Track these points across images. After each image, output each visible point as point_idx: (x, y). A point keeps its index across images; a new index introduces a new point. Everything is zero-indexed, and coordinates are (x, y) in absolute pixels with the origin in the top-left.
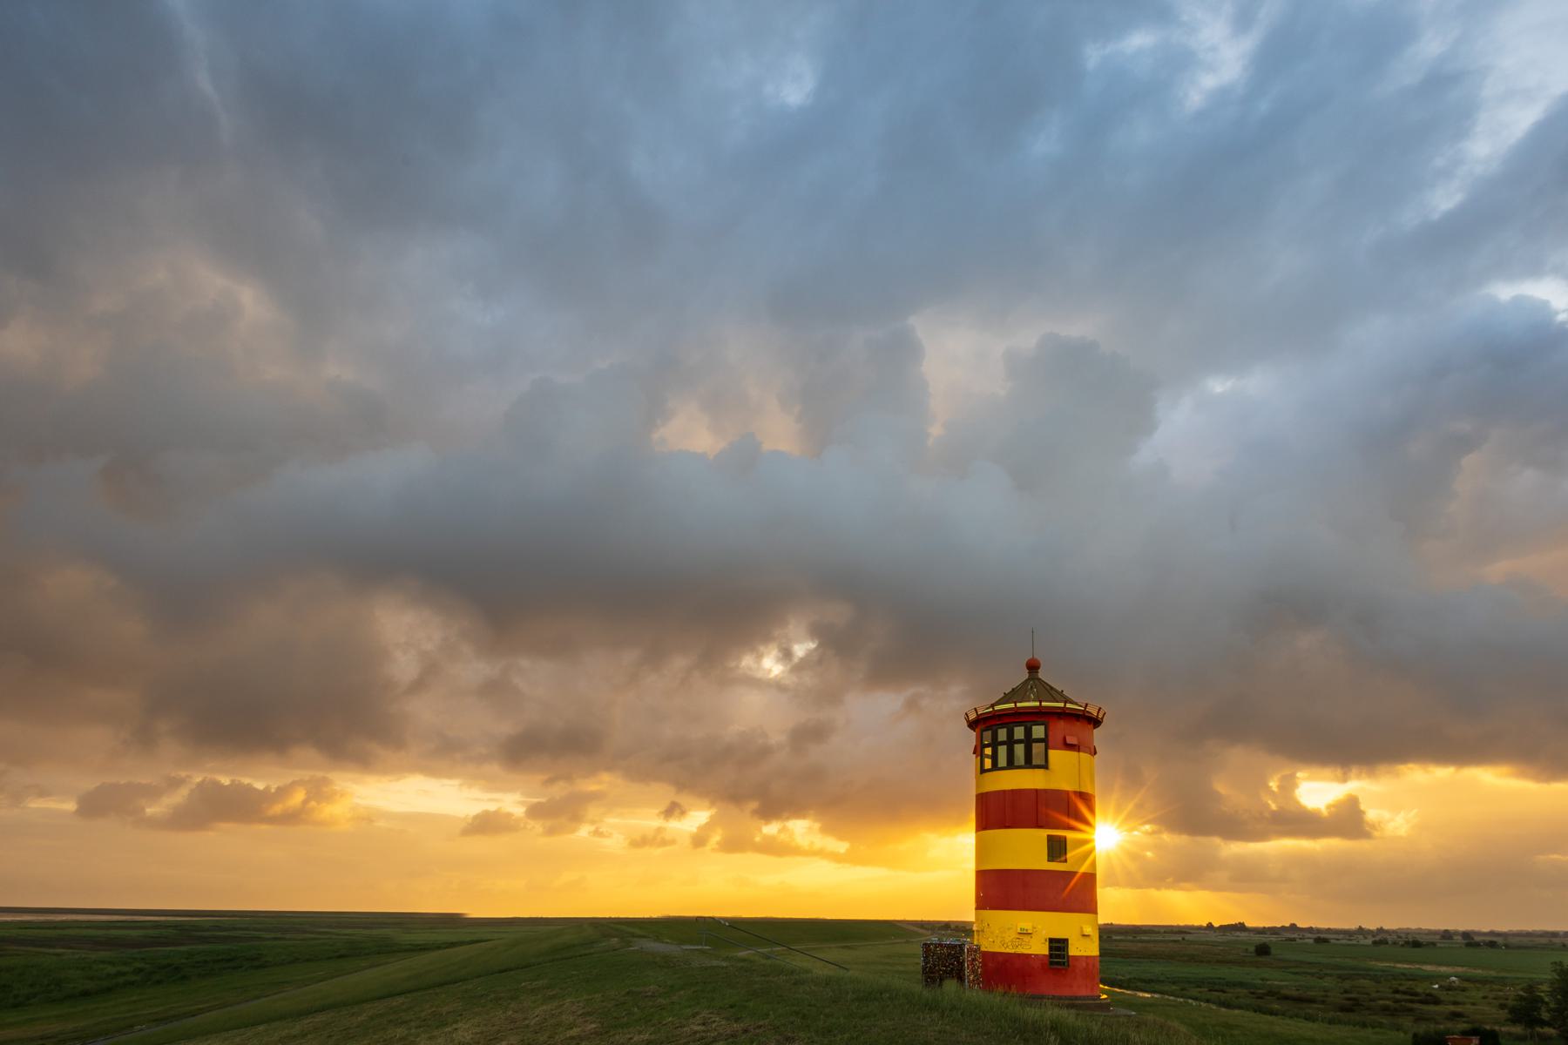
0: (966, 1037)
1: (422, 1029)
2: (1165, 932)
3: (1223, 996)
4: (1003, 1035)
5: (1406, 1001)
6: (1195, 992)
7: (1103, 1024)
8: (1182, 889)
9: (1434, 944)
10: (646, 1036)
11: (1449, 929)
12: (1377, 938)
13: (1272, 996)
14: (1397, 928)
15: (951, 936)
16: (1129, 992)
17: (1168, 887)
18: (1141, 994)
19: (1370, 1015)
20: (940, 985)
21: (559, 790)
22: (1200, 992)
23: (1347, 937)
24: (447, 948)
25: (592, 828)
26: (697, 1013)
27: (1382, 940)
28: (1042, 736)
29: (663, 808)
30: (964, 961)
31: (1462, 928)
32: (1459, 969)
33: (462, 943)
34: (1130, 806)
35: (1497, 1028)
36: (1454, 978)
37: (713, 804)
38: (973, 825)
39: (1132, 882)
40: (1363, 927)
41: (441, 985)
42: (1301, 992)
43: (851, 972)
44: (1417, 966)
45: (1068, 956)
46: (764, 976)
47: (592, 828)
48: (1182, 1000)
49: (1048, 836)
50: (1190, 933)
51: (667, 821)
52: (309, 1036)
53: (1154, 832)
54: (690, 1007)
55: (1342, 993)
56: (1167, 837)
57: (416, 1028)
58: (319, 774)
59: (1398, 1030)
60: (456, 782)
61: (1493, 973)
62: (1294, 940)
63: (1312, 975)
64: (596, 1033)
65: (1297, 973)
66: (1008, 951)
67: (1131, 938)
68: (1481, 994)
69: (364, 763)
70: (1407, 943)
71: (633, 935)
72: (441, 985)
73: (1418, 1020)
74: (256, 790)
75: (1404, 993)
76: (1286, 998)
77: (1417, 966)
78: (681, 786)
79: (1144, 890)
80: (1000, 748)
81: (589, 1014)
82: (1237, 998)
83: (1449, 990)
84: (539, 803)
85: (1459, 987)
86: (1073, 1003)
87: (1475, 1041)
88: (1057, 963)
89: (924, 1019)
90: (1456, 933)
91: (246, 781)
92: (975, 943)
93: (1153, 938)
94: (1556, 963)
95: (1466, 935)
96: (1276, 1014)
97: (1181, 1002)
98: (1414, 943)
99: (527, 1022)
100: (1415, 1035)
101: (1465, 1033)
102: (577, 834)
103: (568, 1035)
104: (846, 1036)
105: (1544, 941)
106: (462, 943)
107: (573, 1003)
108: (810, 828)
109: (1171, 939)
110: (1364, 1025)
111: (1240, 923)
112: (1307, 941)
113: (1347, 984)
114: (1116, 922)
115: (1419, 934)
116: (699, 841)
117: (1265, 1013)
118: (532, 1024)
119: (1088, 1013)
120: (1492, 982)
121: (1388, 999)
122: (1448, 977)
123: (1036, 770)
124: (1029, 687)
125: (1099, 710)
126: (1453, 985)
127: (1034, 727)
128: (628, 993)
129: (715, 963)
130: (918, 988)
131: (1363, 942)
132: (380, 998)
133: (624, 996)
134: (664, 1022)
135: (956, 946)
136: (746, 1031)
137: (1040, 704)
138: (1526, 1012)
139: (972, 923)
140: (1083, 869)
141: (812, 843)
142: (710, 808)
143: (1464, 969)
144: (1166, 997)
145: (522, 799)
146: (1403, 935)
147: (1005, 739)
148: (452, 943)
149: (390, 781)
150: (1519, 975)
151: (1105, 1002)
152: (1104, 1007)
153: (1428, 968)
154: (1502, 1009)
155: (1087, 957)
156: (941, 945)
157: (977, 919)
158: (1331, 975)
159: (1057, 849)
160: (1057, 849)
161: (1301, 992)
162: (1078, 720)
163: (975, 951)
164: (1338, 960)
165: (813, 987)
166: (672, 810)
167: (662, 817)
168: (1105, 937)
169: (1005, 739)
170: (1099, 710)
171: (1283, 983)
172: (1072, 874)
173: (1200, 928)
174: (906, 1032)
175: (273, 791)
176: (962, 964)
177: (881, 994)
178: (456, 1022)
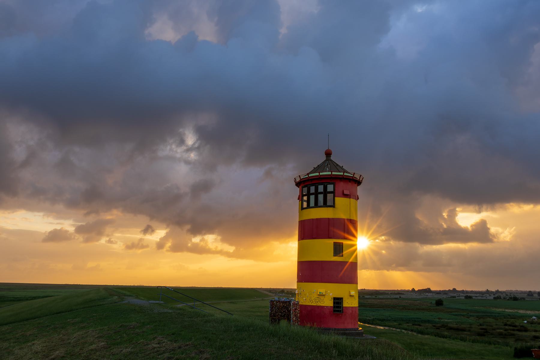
1: (16, 344)
2: (391, 294)
3: (420, 328)
4: (309, 350)
5: (511, 330)
6: (405, 326)
9: (524, 299)
10: (129, 350)
11: (531, 290)
12: (496, 296)
13: (444, 328)
14: (505, 290)
15: (284, 296)
16: (373, 326)
17: (393, 270)
18: (379, 327)
19: (493, 337)
20: (279, 323)
21: (92, 219)
22: (408, 326)
24: (31, 300)
26: (156, 337)
27: (498, 296)
28: (332, 190)
29: (143, 228)
30: (290, 310)
32: (537, 312)
33: (39, 297)
34: (375, 226)
36: (534, 317)
37: (168, 226)
38: (296, 237)
39: (375, 267)
41: (27, 320)
42: (458, 325)
43: (234, 316)
44: (516, 311)
45: (343, 307)
46: (190, 317)
47: (108, 239)
49: (334, 243)
50: (403, 294)
51: (145, 235)
53: (386, 240)
54: (152, 334)
55: (478, 326)
56: (392, 242)
59: (507, 346)
60: (41, 214)
62: (455, 297)
63: (463, 315)
64: (104, 347)
66: (313, 304)
67: (374, 297)
70: (511, 298)
71: (125, 295)
72: (27, 320)
73: (517, 340)
75: (510, 325)
76: (451, 328)
77: (516, 311)
78: (152, 217)
79: (381, 271)
81: (101, 337)
82: (426, 329)
84: (82, 226)
85: (537, 322)
86: (345, 333)
88: (338, 311)
90: (535, 292)
92: (297, 300)
93: (385, 297)
96: (446, 338)
97: (398, 331)
99: (69, 341)
100: (516, 349)
102: (99, 242)
103: (90, 348)
104: (231, 350)
106: (39, 297)
107: (93, 331)
108: (215, 239)
109: (394, 297)
110: (490, 343)
111: (428, 288)
112: (461, 297)
113: (481, 321)
114: (366, 288)
115: (517, 293)
116: (160, 246)
117: (440, 337)
118: (72, 342)
119: (352, 338)
121: (501, 329)
122: (531, 316)
124: (326, 164)
125: (360, 176)
126: (534, 320)
128: (121, 326)
129: (166, 310)
130: (267, 324)
131: (489, 298)
133: (119, 328)
134: (139, 342)
135: (287, 302)
136: (180, 347)
137: (332, 173)
139: (295, 290)
140: (351, 260)
141: (217, 247)
142: (166, 228)
144: (391, 328)
145: (73, 223)
146: (508, 294)
147: (314, 192)
148: (34, 297)
149: (9, 213)
151: (361, 331)
152: (360, 334)
153: (521, 312)
155: (352, 307)
156: (279, 301)
157: (298, 287)
158: (473, 316)
160: (338, 249)
161: (458, 325)
162: (350, 182)
163: (297, 305)
164: (476, 307)
165: (214, 324)
166: (148, 230)
167: (143, 232)
169: (314, 192)
170: (360, 176)
171: (449, 321)
172: (344, 263)
173: (408, 291)
176: (289, 311)
178: (34, 340)
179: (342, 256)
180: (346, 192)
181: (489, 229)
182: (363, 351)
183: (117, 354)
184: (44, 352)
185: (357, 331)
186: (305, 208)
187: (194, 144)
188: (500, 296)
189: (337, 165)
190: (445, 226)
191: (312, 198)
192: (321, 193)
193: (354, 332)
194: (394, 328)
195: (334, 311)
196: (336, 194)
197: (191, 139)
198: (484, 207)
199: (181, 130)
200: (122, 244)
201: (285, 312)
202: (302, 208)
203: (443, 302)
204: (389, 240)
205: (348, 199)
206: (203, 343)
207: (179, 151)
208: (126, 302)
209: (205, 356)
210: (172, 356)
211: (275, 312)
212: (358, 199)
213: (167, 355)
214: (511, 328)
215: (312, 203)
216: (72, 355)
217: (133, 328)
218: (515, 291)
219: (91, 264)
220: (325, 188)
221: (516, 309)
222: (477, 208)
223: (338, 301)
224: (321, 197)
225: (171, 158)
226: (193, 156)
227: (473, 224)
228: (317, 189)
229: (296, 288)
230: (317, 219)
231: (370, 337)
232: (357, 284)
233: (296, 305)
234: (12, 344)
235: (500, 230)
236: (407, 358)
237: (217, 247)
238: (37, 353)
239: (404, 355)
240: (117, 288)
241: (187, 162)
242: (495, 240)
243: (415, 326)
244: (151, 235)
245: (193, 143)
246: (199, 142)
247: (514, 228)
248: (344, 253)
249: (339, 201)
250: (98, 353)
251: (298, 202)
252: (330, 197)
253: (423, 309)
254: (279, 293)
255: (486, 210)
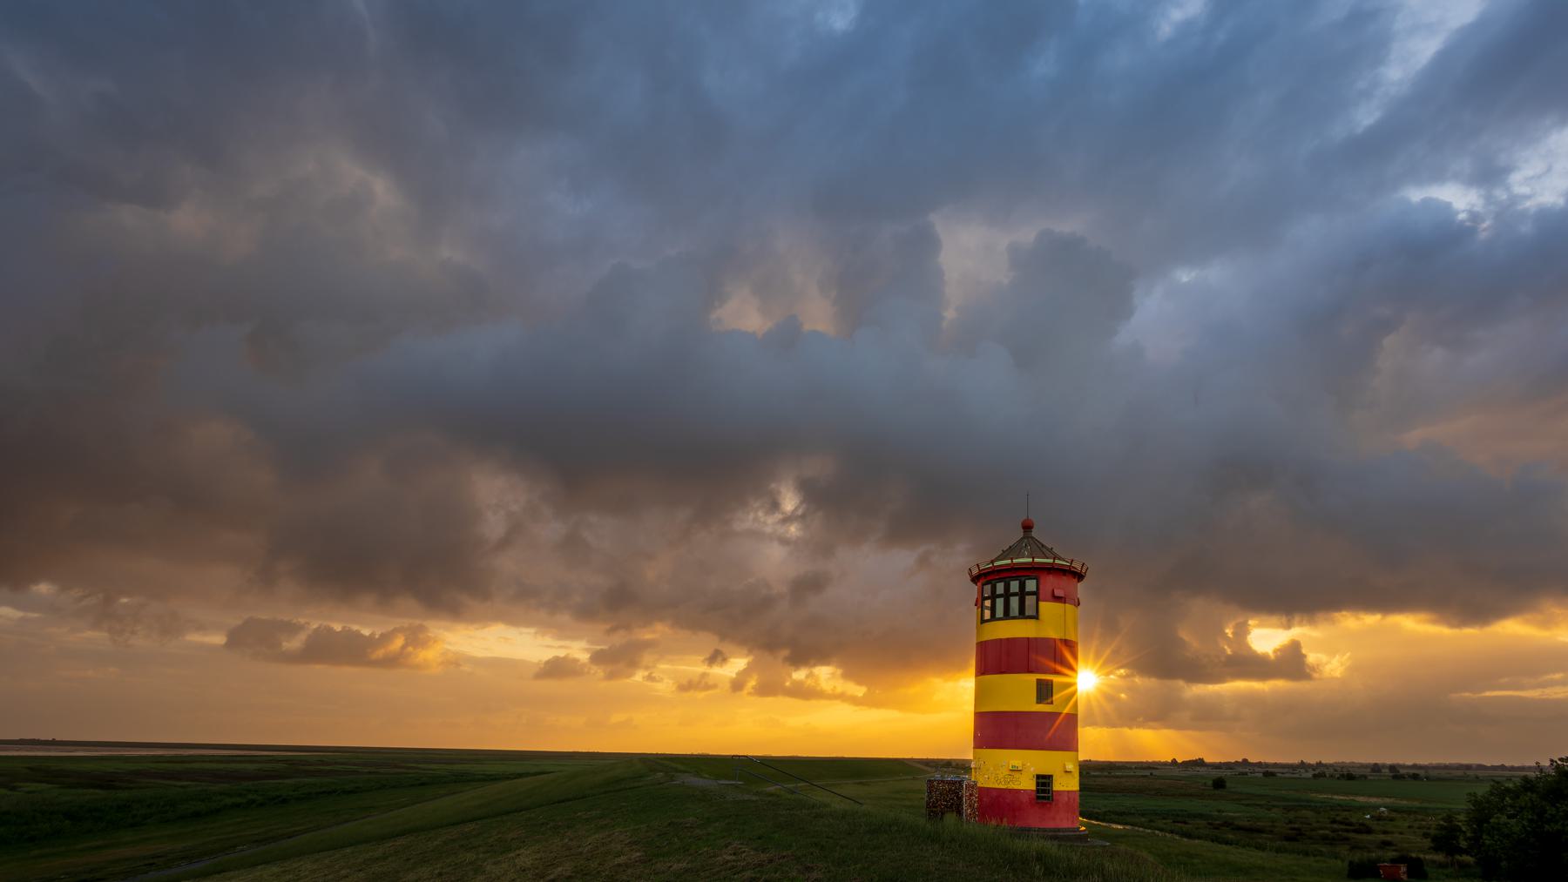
0: (963, 867)
1: (489, 854)
2: (1136, 768)
3: (1185, 827)
4: (995, 865)
5: (1342, 830)
7: (1082, 854)
8: (1149, 728)
11: (1378, 762)
12: (1317, 772)
16: (1104, 824)
17: (1139, 726)
18: (1114, 826)
20: (942, 819)
21: (619, 639)
22: (1165, 824)
23: (1291, 771)
25: (646, 673)
26: (730, 844)
27: (1321, 773)
29: (708, 656)
31: (1389, 762)
32: (1388, 800)
34: (1108, 652)
35: (1422, 856)
36: (1383, 809)
37: (750, 652)
38: (972, 670)
39: (1109, 723)
40: (1305, 761)
41: (508, 813)
47: (646, 673)
48: (1149, 831)
49: (1038, 680)
50: (1157, 769)
52: (390, 859)
53: (1127, 676)
54: (724, 837)
56: (1137, 680)
57: (484, 853)
58: (417, 622)
59: (1336, 858)
60: (532, 630)
61: (1417, 804)
62: (1246, 774)
65: (1248, 805)
66: (1001, 786)
67: (1106, 774)
68: (1406, 824)
69: (455, 612)
70: (1343, 776)
71: (677, 771)
72: (508, 813)
73: (1354, 848)
74: (362, 636)
75: (1341, 823)
76: (1239, 828)
78: (723, 636)
80: (998, 600)
81: (635, 843)
82: (1197, 829)
83: (1379, 820)
84: (602, 650)
87: (1403, 868)
88: (1044, 798)
89: (927, 850)
90: (1384, 766)
91: (355, 627)
92: (973, 780)
93: (1125, 774)
94: (1470, 794)
95: (1393, 768)
96: (1231, 844)
97: (1149, 833)
98: (1348, 776)
99: (580, 850)
100: (1351, 863)
101: (1393, 861)
102: (633, 678)
104: (859, 866)
105: (1460, 773)
106: (527, 775)
108: (833, 674)
110: (1307, 854)
113: (1292, 815)
116: (737, 685)
117: (1220, 843)
119: (1069, 844)
120: (1415, 812)
121: (1326, 829)
123: (1028, 620)
127: (1027, 581)
128: (669, 824)
129: (746, 797)
132: (453, 824)
136: (771, 861)
138: (1445, 840)
139: (969, 761)
140: (1066, 711)
141: (835, 687)
142: (747, 655)
143: (1392, 800)
144: (1136, 828)
145: (587, 646)
146: (1339, 769)
149: (477, 629)
150: (1439, 805)
151: (1082, 833)
152: (1082, 838)
153: (1361, 799)
154: (1426, 838)
155: (1068, 791)
159: (1045, 691)
160: (1045, 691)
162: (1065, 575)
164: (1283, 792)
166: (716, 657)
167: (707, 662)
168: (1084, 773)
172: (1056, 715)
173: (1165, 764)
174: (911, 862)
175: (377, 637)
176: (960, 799)
177: (890, 826)
178: (519, 848)
179: (1052, 703)
180: (1058, 593)
181: (1305, 656)
182: (1088, 868)
183: (663, 872)
184: (537, 868)
185: (1078, 833)
186: (987, 621)
187: (796, 509)
188: (1324, 773)
189: (1043, 546)
190: (1229, 652)
191: (1000, 602)
192: (1015, 594)
193: (1072, 833)
194: (1139, 827)
195: (1038, 798)
196: (1041, 596)
197: (790, 502)
198: (1297, 618)
199: (773, 486)
200: (671, 682)
201: (953, 799)
202: (983, 621)
203: (1225, 782)
204: (1132, 675)
205: (1061, 605)
206: (812, 854)
207: (770, 522)
208: (678, 782)
209: (815, 875)
210: (758, 875)
211: (937, 799)
212: (1079, 604)
213: (748, 874)
214: (1343, 827)
215: (1000, 612)
216: (586, 874)
217: (691, 827)
218: (1350, 763)
219: (617, 718)
220: (1022, 586)
221: (1352, 794)
222: (1284, 619)
223: (1044, 781)
224: (1014, 602)
225: (757, 535)
226: (793, 530)
227: (1278, 647)
228: (1007, 588)
229: (972, 758)
230: (1008, 639)
231: (1100, 842)
232: (1077, 750)
233: (973, 787)
234: (481, 856)
235: (1323, 657)
236: (1164, 879)
237: (835, 687)
238: (524, 870)
239: (1158, 874)
240: (662, 759)
241: (784, 541)
242: (1316, 675)
243: (1180, 825)
244: (721, 666)
245: (793, 508)
246: (804, 506)
247: (1348, 654)
248: (1055, 697)
249: (1045, 607)
250: (629, 871)
251: (975, 611)
252: (1030, 600)
253: (1191, 795)
254: (943, 766)
255: (1301, 624)
